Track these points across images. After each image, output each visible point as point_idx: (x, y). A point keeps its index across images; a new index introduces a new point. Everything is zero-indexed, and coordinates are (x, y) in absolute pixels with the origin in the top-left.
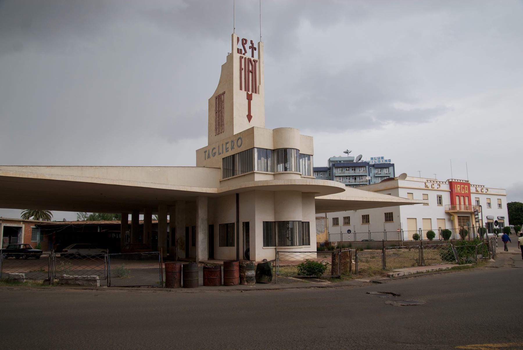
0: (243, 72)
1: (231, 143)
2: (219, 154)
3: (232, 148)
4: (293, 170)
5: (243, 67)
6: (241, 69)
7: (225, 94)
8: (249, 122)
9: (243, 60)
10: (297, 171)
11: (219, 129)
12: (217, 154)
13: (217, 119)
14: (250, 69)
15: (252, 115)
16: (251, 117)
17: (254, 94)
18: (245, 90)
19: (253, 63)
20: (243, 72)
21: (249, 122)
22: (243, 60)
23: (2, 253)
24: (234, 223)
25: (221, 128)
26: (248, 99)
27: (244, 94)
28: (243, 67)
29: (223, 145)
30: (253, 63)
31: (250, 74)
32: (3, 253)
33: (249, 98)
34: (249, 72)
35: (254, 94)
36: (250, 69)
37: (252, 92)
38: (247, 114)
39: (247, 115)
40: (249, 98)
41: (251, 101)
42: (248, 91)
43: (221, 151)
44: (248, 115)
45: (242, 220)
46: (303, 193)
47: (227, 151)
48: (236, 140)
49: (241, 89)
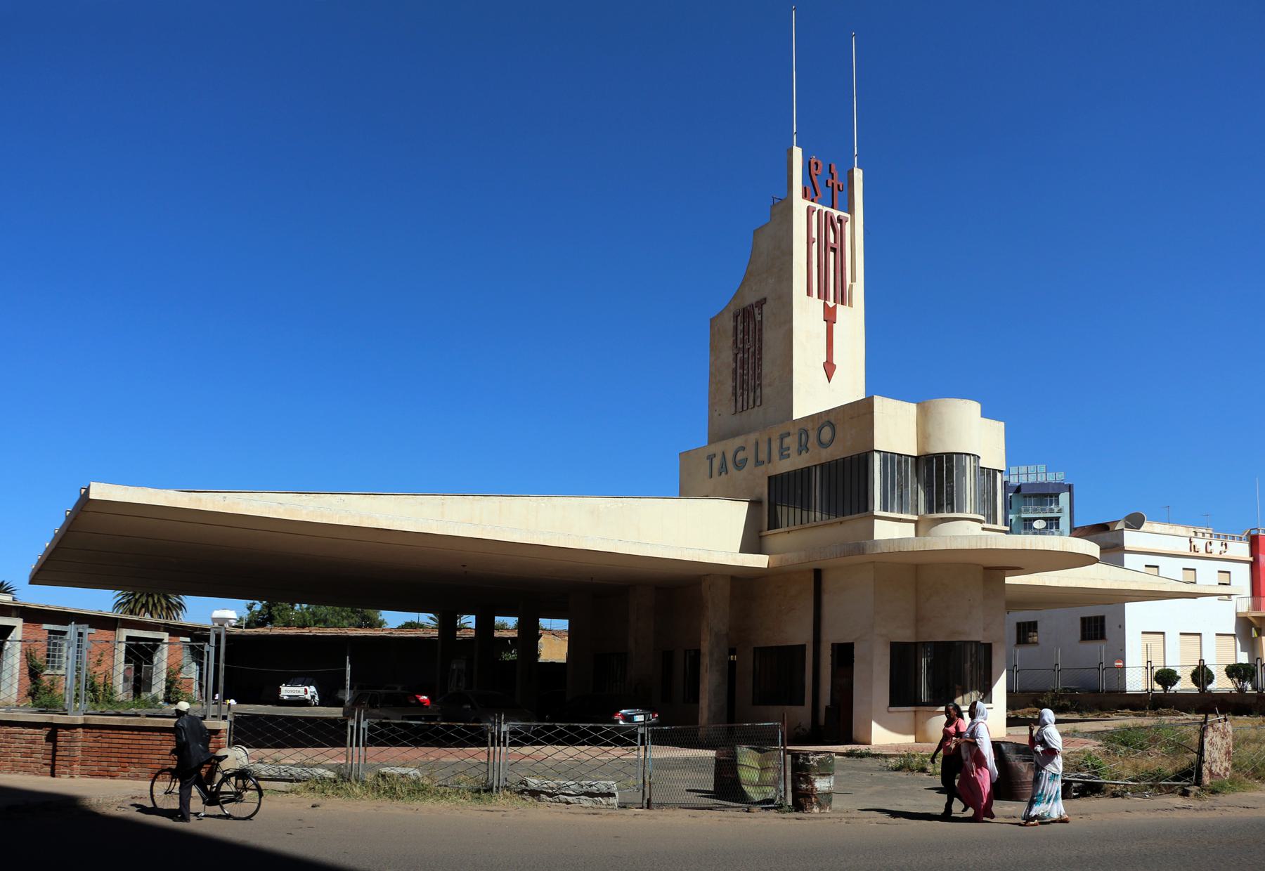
1: (797, 437)
2: (758, 463)
3: (803, 448)
7: (764, 306)
11: (745, 396)
12: (751, 462)
13: (739, 371)
14: (832, 240)
15: (835, 363)
16: (834, 367)
17: (839, 307)
23: (364, 720)
24: (803, 647)
25: (751, 395)
26: (826, 321)
27: (817, 305)
28: (815, 235)
29: (770, 440)
31: (832, 254)
32: (367, 720)
33: (830, 317)
34: (829, 249)
35: (839, 307)
36: (832, 240)
38: (825, 360)
40: (830, 317)
42: (826, 298)
43: (763, 456)
45: (831, 636)
46: (986, 568)
47: (784, 454)
48: (813, 429)
49: (809, 293)
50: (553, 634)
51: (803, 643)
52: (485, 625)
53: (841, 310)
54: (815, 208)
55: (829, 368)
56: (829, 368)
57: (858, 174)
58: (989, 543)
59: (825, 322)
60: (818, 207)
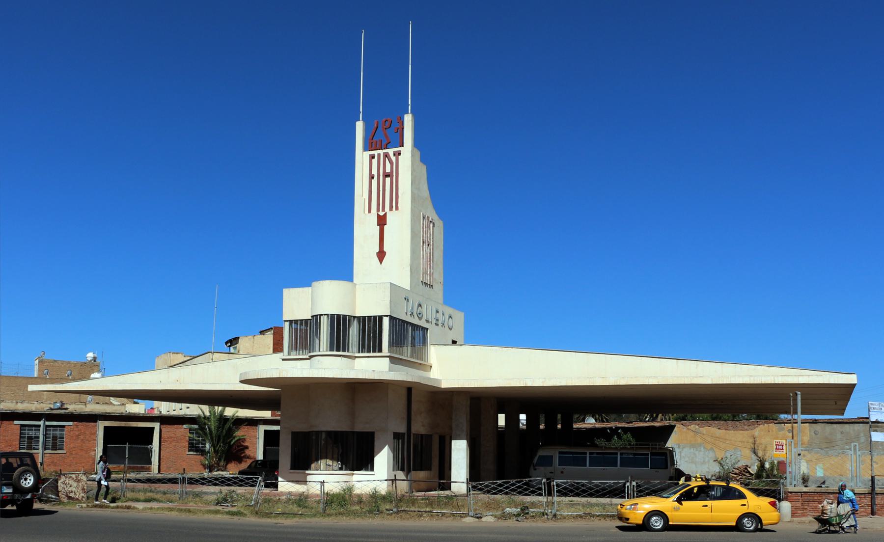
0: (375, 181)
4: (321, 350)
5: (375, 172)
6: (372, 177)
8: (381, 264)
9: (375, 161)
10: (331, 349)
15: (385, 250)
18: (378, 210)
19: (394, 159)
20: (375, 181)
21: (381, 264)
22: (375, 161)
28: (375, 172)
30: (394, 159)
33: (382, 221)
36: (388, 170)
37: (391, 209)
38: (378, 251)
39: (377, 253)
40: (382, 221)
41: (385, 226)
42: (383, 210)
44: (379, 252)
49: (370, 211)
50: (682, 424)
51: (373, 431)
52: (512, 420)
53: (391, 217)
54: (374, 155)
55: (381, 255)
56: (381, 255)
57: (408, 119)
58: (268, 374)
59: (378, 226)
60: (376, 152)
